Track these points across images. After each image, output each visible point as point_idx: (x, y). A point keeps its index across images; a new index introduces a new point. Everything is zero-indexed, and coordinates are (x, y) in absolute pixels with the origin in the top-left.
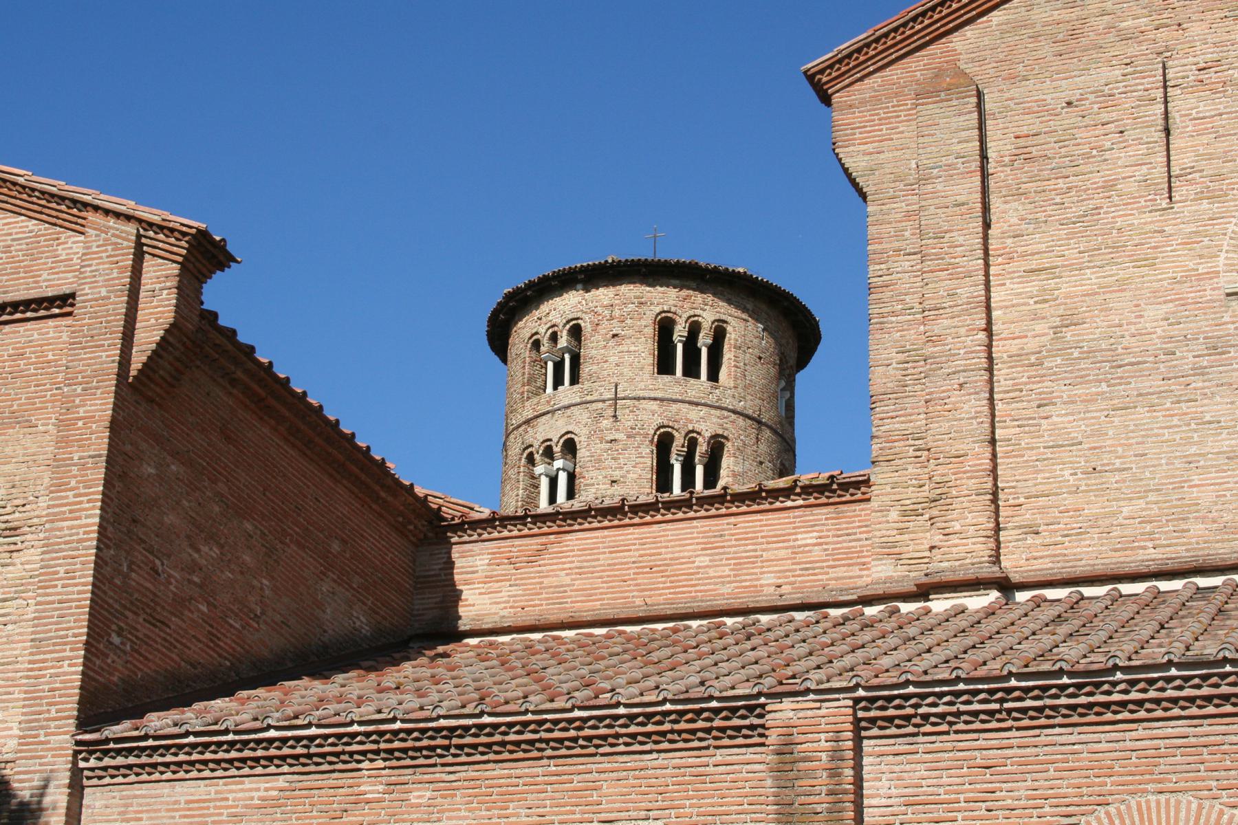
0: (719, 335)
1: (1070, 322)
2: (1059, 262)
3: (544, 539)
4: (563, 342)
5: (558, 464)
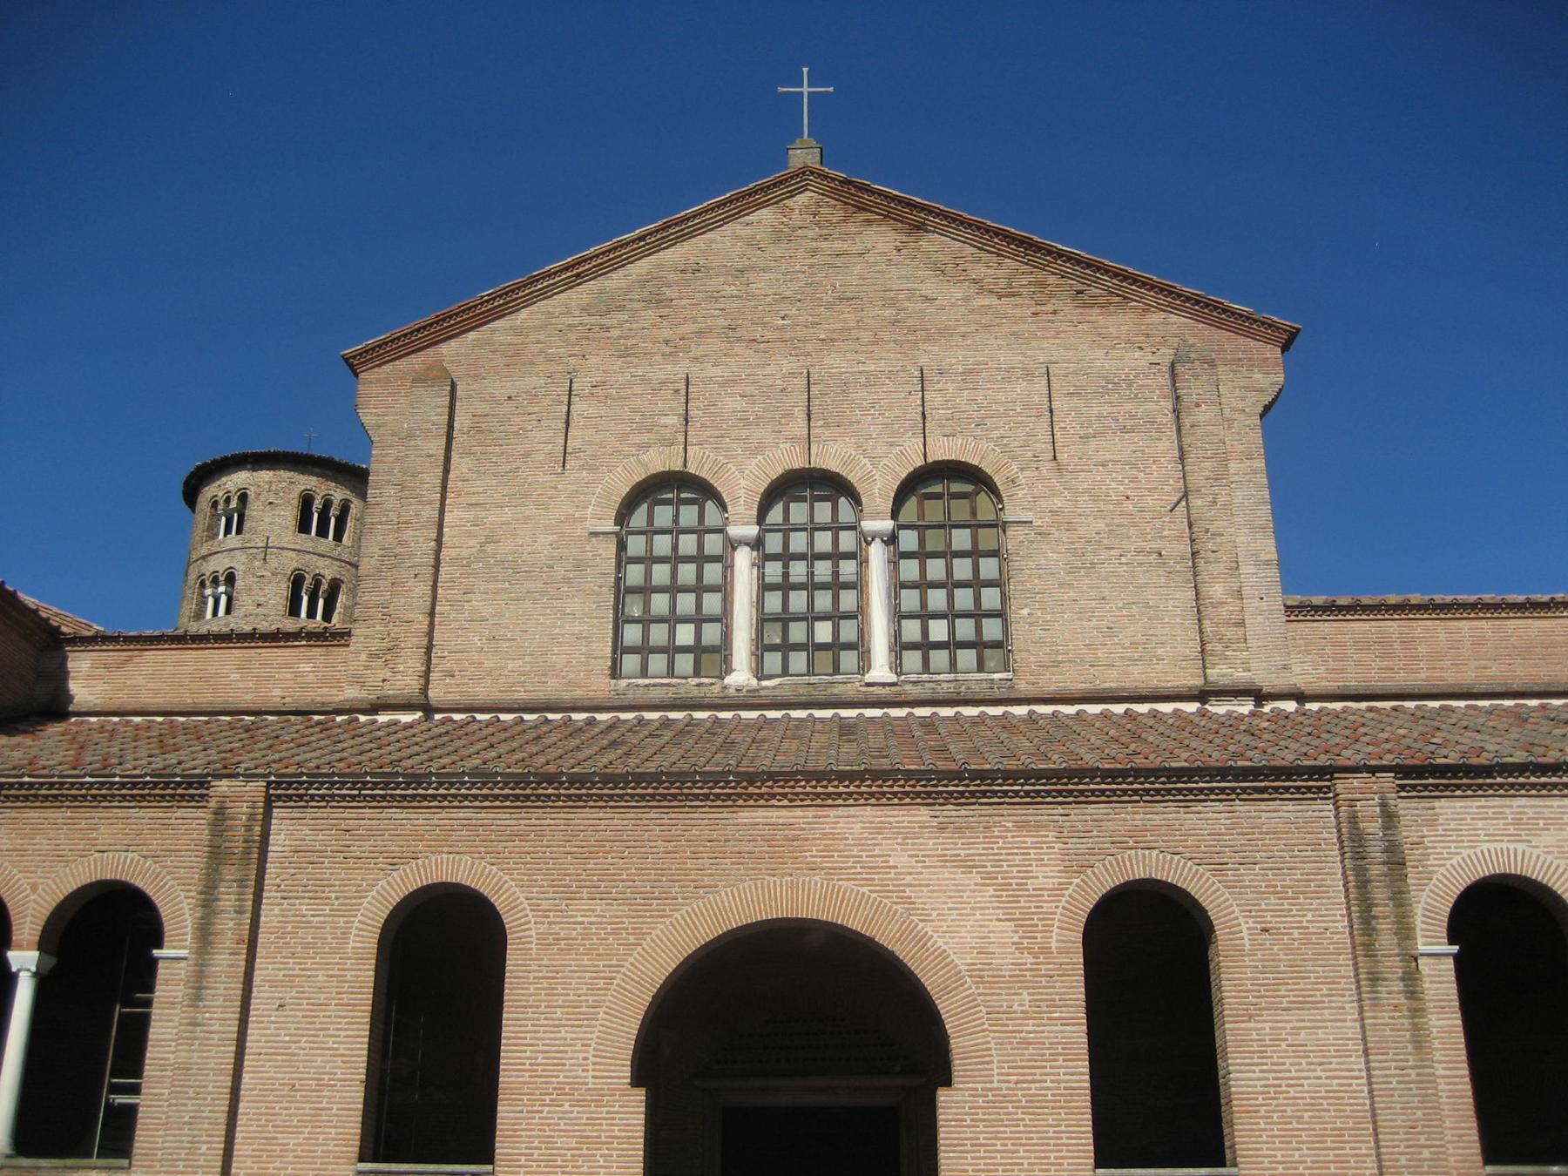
0: (345, 509)
1: (491, 540)
2: (490, 500)
3: (130, 653)
4: (233, 504)
5: (222, 589)
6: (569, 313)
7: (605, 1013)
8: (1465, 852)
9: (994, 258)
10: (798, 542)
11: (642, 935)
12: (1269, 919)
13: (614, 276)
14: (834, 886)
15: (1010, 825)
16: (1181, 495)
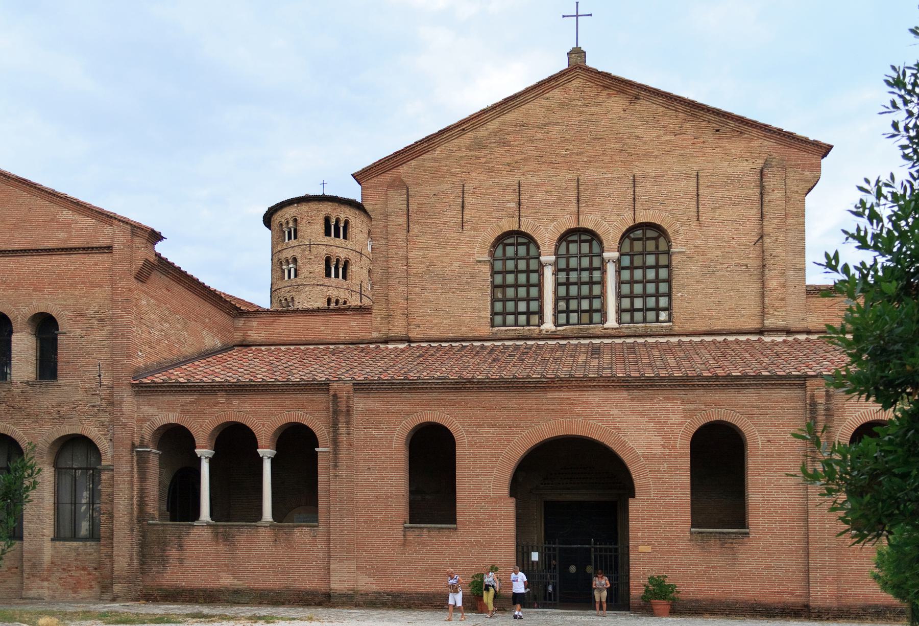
2: (429, 246)
6: (460, 150)
7: (496, 470)
8: (862, 411)
10: (573, 263)
11: (509, 441)
12: (771, 437)
13: (481, 129)
14: (587, 422)
15: (661, 398)
16: (760, 236)
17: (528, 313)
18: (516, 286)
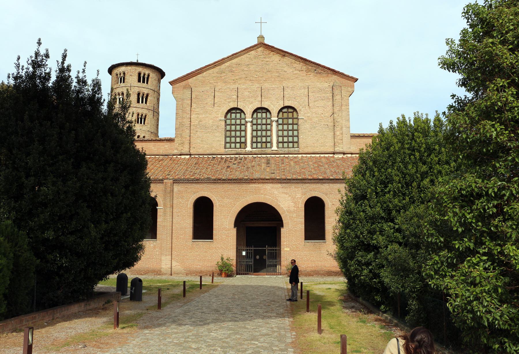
0: (149, 75)
9: (299, 62)
10: (259, 121)
17: (240, 143)
18: (236, 131)
